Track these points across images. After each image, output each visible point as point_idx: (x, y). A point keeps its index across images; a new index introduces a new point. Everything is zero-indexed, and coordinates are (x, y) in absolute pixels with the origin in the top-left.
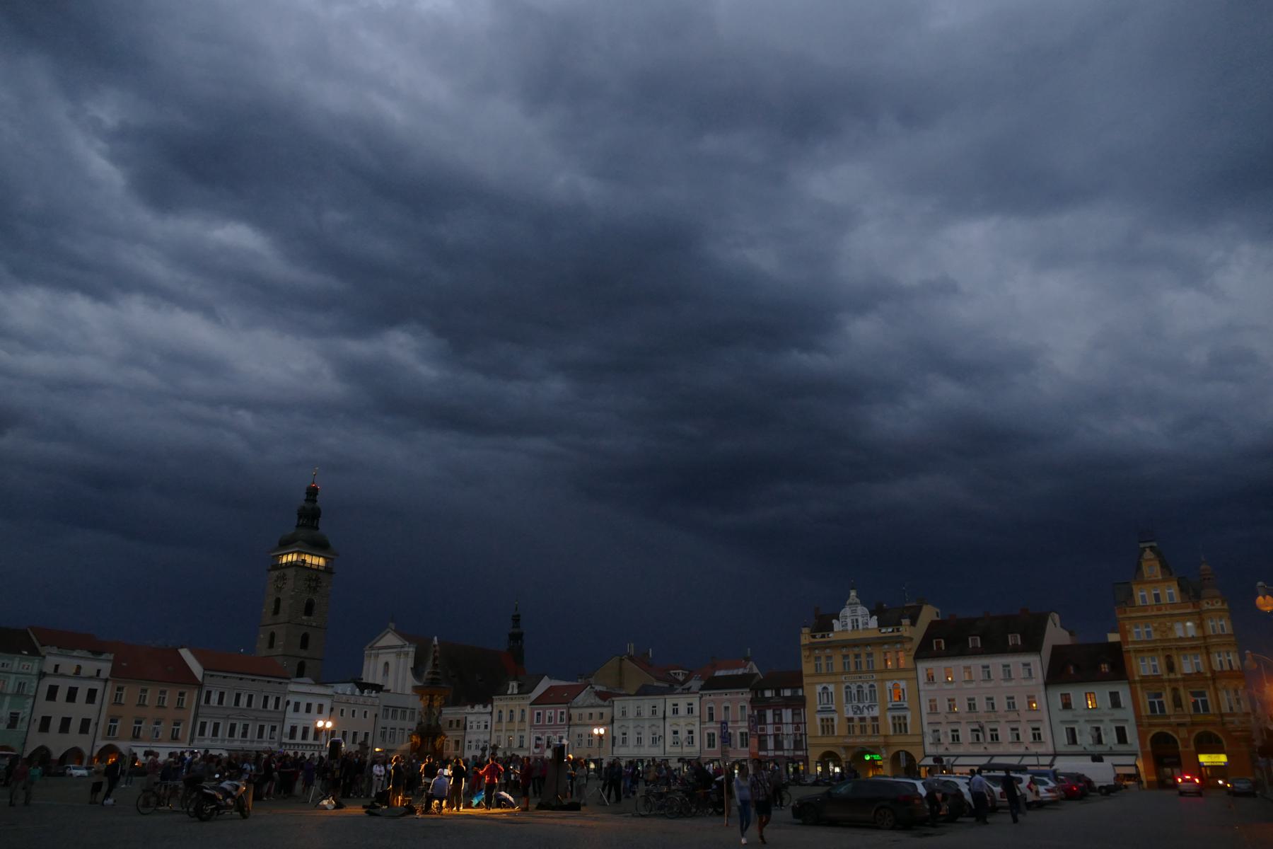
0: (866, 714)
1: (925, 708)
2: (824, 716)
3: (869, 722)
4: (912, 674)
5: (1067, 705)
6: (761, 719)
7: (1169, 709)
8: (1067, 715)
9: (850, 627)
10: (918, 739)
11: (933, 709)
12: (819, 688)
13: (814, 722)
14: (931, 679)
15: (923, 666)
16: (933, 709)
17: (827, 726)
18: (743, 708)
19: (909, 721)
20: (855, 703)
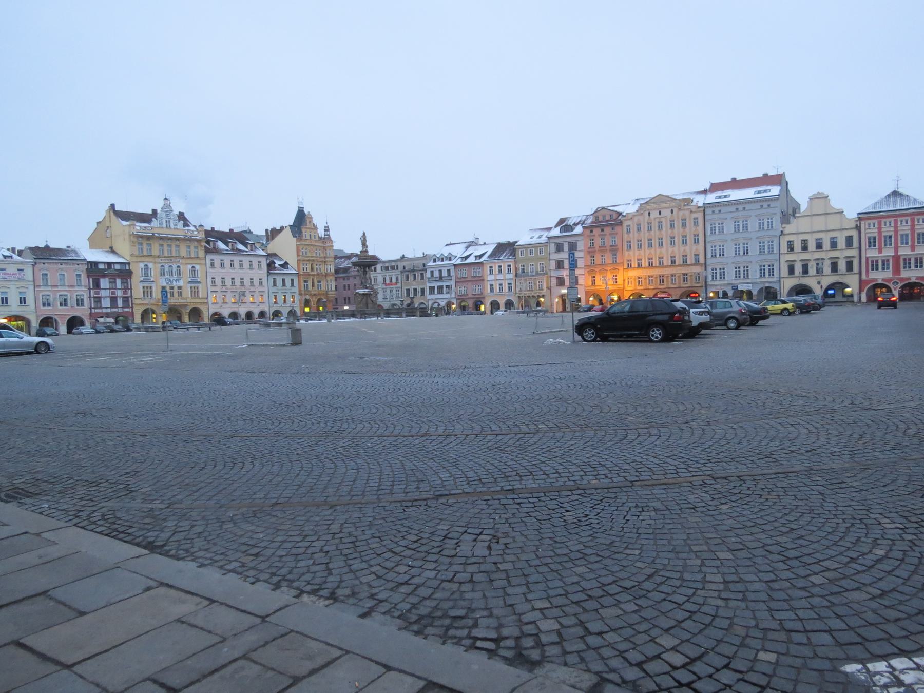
0: (174, 284)
1: (210, 283)
2: (146, 285)
3: (176, 290)
4: (203, 262)
5: (275, 285)
6: (97, 285)
7: (310, 288)
8: (274, 289)
9: (164, 225)
10: (205, 301)
11: (214, 283)
12: (142, 265)
13: (137, 291)
14: (212, 265)
15: (209, 257)
16: (214, 283)
17: (147, 292)
18: (79, 276)
19: (200, 289)
20: (167, 277)
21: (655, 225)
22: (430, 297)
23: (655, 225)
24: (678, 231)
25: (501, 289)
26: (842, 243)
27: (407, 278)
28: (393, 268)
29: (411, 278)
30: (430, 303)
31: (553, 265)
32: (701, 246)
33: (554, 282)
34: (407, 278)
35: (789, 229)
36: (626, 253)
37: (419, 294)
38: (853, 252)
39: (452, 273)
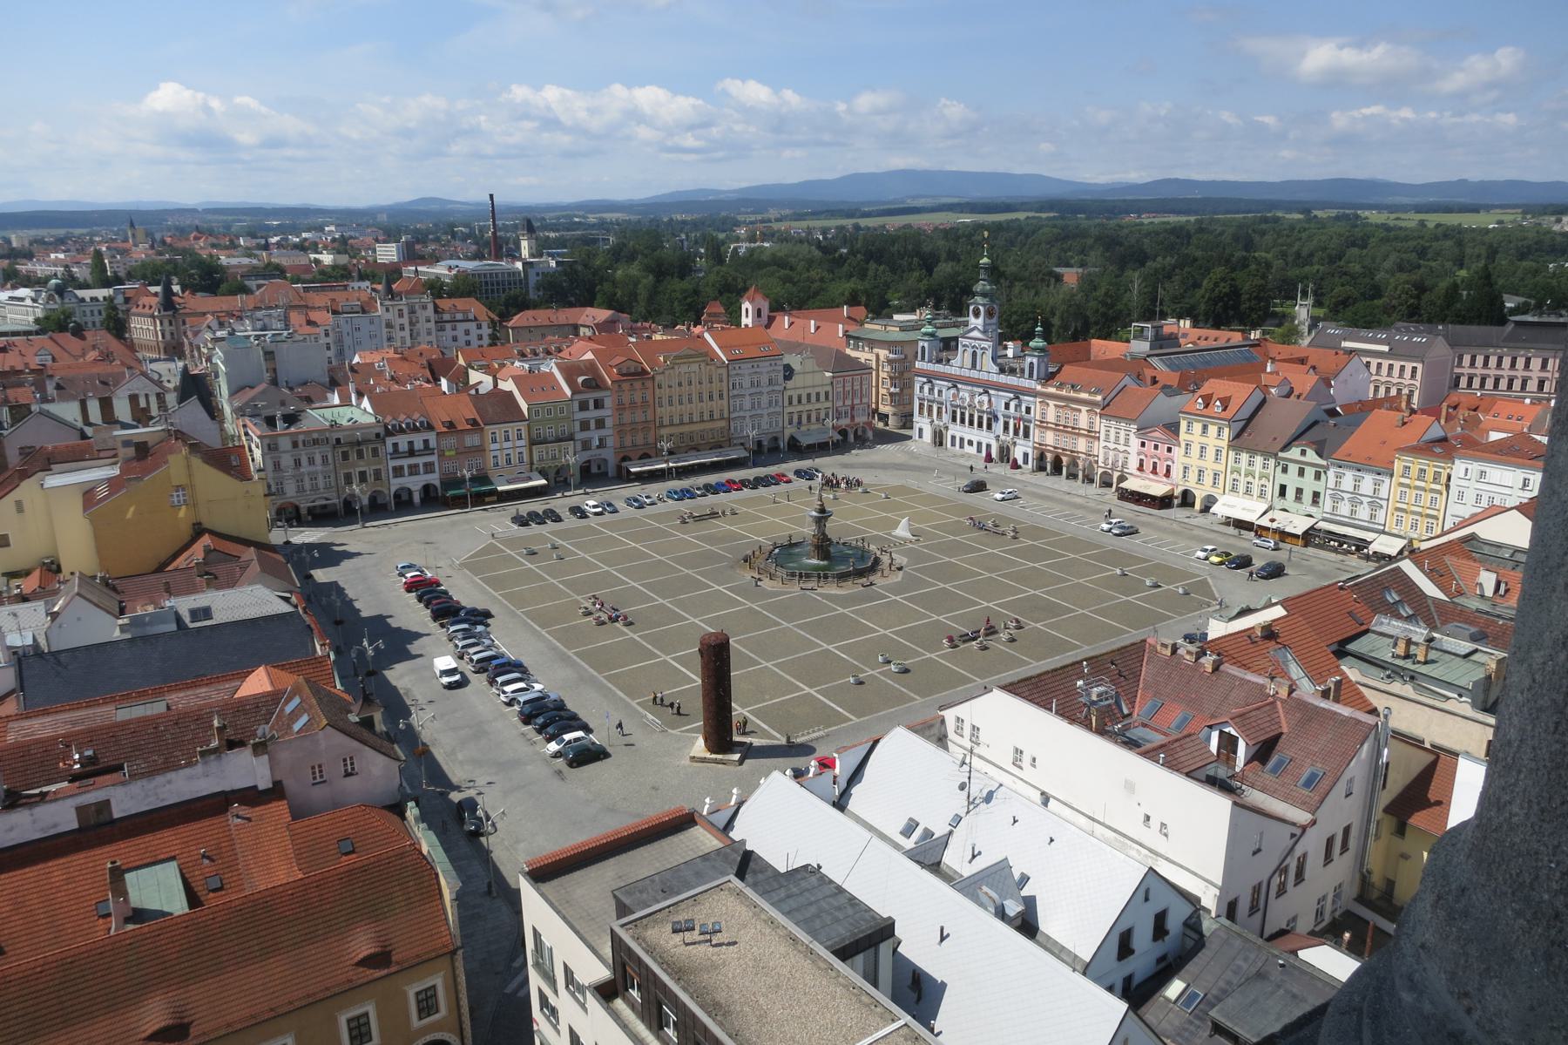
21: (685, 383)
22: (393, 481)
23: (685, 383)
24: (706, 386)
25: (509, 462)
26: (822, 397)
27: (345, 456)
28: (316, 442)
29: (353, 456)
30: (393, 489)
31: (577, 425)
32: (725, 402)
33: (579, 447)
34: (345, 456)
35: (790, 384)
36: (658, 410)
37: (371, 479)
38: (829, 404)
39: (433, 444)
